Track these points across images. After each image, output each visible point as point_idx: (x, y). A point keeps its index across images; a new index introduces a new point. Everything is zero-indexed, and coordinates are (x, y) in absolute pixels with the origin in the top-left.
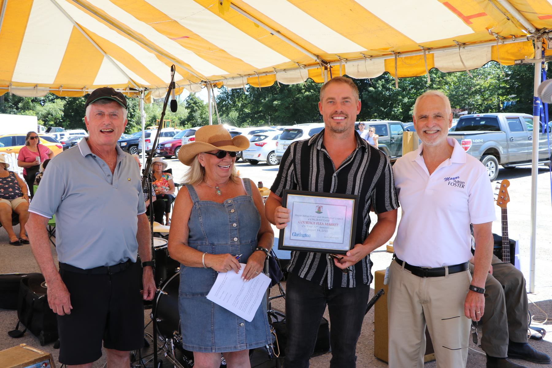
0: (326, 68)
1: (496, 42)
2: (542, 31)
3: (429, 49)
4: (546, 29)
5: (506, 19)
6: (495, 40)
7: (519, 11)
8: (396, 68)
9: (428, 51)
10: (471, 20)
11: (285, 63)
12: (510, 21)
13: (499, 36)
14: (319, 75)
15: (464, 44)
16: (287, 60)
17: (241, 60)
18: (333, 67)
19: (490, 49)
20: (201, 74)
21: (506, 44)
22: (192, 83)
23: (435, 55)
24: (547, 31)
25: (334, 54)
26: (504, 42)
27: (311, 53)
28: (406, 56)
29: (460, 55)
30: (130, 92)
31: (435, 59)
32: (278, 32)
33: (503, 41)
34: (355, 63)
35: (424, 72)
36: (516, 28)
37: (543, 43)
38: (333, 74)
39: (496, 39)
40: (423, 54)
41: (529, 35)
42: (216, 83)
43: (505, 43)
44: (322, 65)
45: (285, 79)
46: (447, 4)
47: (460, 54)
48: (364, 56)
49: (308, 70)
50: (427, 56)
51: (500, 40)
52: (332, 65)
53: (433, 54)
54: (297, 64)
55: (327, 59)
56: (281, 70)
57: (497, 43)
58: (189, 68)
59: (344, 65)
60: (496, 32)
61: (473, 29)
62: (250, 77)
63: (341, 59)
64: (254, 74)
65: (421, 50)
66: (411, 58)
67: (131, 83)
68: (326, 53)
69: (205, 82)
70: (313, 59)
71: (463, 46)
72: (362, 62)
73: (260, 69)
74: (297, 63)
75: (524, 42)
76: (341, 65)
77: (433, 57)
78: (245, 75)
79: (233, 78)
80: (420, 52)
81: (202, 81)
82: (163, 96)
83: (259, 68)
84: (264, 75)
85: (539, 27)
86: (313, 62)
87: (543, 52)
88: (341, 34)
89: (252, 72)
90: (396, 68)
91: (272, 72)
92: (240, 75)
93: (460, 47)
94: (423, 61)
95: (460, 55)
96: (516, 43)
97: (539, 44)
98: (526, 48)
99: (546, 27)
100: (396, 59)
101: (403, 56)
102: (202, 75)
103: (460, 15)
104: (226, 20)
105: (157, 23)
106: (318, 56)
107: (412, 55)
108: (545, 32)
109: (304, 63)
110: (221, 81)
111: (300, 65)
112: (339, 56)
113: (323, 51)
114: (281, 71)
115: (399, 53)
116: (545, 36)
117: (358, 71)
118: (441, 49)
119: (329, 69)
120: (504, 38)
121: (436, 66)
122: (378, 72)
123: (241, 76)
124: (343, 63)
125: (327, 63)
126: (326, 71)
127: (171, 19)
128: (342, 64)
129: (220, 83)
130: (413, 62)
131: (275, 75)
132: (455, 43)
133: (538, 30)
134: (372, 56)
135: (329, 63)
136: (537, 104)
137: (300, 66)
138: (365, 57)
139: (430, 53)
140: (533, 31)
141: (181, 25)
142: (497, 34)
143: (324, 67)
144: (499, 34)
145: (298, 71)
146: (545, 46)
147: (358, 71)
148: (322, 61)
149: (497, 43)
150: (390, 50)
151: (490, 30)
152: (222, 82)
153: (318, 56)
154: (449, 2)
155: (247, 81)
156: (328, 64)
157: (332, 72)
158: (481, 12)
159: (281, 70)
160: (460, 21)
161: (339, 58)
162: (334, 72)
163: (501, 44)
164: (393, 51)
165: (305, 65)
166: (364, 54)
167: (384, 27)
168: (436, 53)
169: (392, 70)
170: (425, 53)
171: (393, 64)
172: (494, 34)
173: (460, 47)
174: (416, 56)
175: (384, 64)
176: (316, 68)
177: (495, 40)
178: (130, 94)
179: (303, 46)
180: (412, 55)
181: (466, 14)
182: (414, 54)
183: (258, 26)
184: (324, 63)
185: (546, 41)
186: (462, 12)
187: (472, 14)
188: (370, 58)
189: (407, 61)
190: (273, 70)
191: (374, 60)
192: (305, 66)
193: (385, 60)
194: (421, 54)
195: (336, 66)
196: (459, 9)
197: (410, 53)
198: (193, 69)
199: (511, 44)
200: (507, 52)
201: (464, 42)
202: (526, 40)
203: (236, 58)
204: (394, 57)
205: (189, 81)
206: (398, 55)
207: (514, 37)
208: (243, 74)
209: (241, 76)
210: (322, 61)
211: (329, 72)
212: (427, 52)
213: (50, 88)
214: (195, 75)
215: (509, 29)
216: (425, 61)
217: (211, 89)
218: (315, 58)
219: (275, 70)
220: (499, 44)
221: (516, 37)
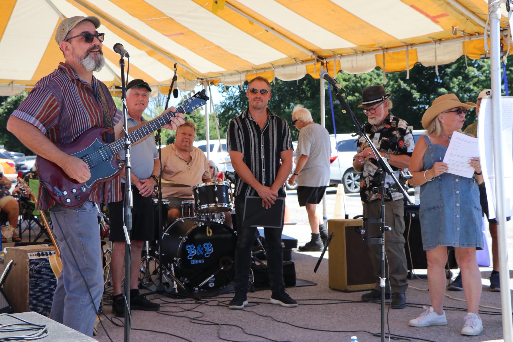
0: (322, 64)
1: (463, 38)
3: (412, 45)
5: (465, 19)
6: (461, 37)
7: (473, 13)
8: (384, 63)
9: (411, 46)
10: (438, 20)
11: (282, 59)
12: (468, 21)
13: (465, 33)
14: (312, 72)
15: (440, 40)
16: (284, 56)
17: (237, 56)
18: (330, 63)
19: (461, 45)
20: (196, 70)
21: (473, 40)
22: (187, 80)
23: (418, 50)
25: (328, 50)
26: (470, 38)
27: (306, 48)
28: (393, 51)
29: (435, 52)
30: (116, 91)
31: (418, 54)
32: (273, 29)
33: (469, 37)
34: (350, 59)
36: (475, 26)
38: (329, 69)
39: (463, 35)
40: (406, 49)
42: (213, 80)
43: (472, 39)
44: (318, 61)
45: (284, 75)
46: (412, 6)
47: (437, 50)
48: (355, 51)
49: (306, 66)
51: (466, 37)
52: (328, 60)
53: (416, 49)
54: (294, 60)
55: (324, 54)
56: (279, 66)
58: (184, 64)
59: (339, 61)
60: (462, 30)
61: (442, 27)
62: (249, 73)
63: (335, 55)
64: (253, 70)
65: (403, 46)
66: (398, 53)
67: (117, 80)
68: (321, 49)
69: (202, 79)
70: (309, 55)
71: (439, 42)
72: (354, 58)
73: (258, 66)
74: (295, 59)
76: (335, 61)
77: (416, 52)
78: (244, 72)
79: (231, 75)
80: (403, 48)
81: (198, 78)
82: (154, 95)
83: (257, 64)
84: (263, 71)
86: (309, 58)
88: (330, 31)
89: (249, 68)
90: (384, 63)
91: (270, 68)
92: (238, 71)
94: (406, 56)
95: (435, 52)
96: (479, 39)
100: (384, 54)
101: (390, 52)
102: (198, 71)
103: (427, 15)
104: (221, 18)
105: (152, 20)
106: (313, 52)
107: (398, 51)
109: (302, 59)
110: (218, 78)
111: (296, 61)
112: (333, 52)
113: (318, 47)
114: (279, 67)
115: (387, 48)
117: (352, 67)
118: (421, 45)
119: (325, 65)
120: (471, 35)
121: (419, 61)
122: (370, 67)
123: (239, 72)
124: (338, 59)
125: (322, 59)
126: (322, 66)
127: (166, 16)
128: (337, 59)
129: (217, 80)
131: (273, 71)
132: (432, 40)
134: (363, 52)
135: (325, 58)
137: (297, 62)
138: (356, 52)
139: (413, 48)
141: (176, 22)
142: (463, 31)
143: (320, 63)
144: (465, 32)
145: (295, 67)
146: (503, 42)
147: (352, 67)
148: (319, 57)
150: (376, 46)
151: (455, 28)
152: (220, 79)
153: (313, 52)
154: (416, 5)
155: (246, 78)
156: (324, 59)
157: (328, 68)
158: (444, 13)
159: (279, 66)
160: (428, 20)
161: (333, 53)
162: (331, 68)
163: (468, 40)
164: (381, 47)
165: (303, 61)
166: (355, 50)
167: (365, 25)
168: (419, 48)
169: (381, 65)
170: (407, 50)
171: (382, 60)
172: (457, 31)
175: (374, 60)
176: (313, 63)
177: (461, 37)
178: (116, 93)
179: (298, 42)
180: (398, 51)
181: (433, 14)
182: (399, 50)
183: (252, 24)
184: (320, 58)
185: (504, 38)
186: (428, 13)
187: (436, 15)
188: (363, 53)
189: (396, 56)
190: (271, 66)
191: (366, 56)
192: (303, 62)
193: (376, 55)
194: (404, 50)
195: (331, 61)
196: (425, 11)
197: (396, 49)
198: (188, 65)
199: (477, 40)
200: (474, 47)
201: (440, 38)
203: (232, 55)
204: (382, 53)
205: (184, 78)
206: (385, 50)
207: (477, 34)
208: (241, 70)
209: (239, 72)
210: (319, 57)
211: (326, 68)
212: (409, 48)
213: (27, 85)
214: (191, 71)
216: (408, 56)
217: (208, 87)
218: (311, 54)
219: (273, 66)
220: (465, 40)
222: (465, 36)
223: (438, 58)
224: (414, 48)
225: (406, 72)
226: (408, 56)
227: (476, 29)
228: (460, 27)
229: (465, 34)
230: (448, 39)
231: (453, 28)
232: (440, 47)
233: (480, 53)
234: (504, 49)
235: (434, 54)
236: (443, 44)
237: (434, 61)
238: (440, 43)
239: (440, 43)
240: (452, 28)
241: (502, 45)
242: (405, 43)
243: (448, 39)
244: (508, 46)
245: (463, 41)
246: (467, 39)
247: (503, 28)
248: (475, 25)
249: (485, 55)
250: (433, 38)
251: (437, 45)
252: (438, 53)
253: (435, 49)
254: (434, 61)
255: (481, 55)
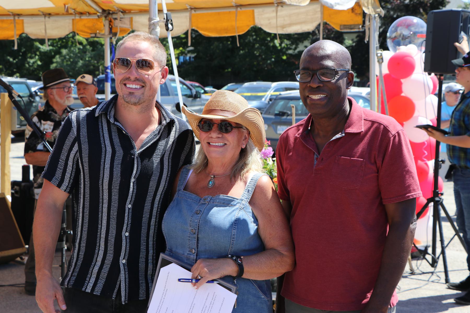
1: (74, 16)
2: (107, 12)
3: (19, 15)
4: (109, 10)
6: (71, 14)
13: (76, 11)
15: (50, 14)
19: (71, 21)
21: (83, 19)
24: (111, 12)
31: (25, 25)
33: (79, 16)
35: (13, 37)
37: (110, 21)
41: (99, 14)
43: (82, 18)
50: (16, 21)
51: (77, 15)
53: (23, 20)
57: (75, 17)
60: (73, 8)
61: (54, 4)
71: (48, 16)
75: (96, 19)
85: (105, 8)
87: (111, 29)
93: (45, 17)
94: (13, 25)
97: (107, 23)
98: (99, 23)
99: (110, 9)
108: (109, 13)
116: (110, 16)
120: (81, 14)
130: (5, 25)
132: (41, 14)
133: (104, 11)
136: (107, 72)
140: (100, 11)
142: (74, 9)
146: (111, 24)
149: (75, 17)
168: (26, 20)
170: (14, 20)
173: (45, 17)
174: (7, 20)
177: (71, 14)
182: (5, 18)
185: (113, 20)
199: (87, 19)
200: (84, 25)
202: (97, 17)
207: (87, 14)
212: (16, 18)
215: (81, 7)
216: (15, 26)
221: (89, 14)
222: (76, 14)
223: (48, 31)
224: (21, 18)
225: (13, 41)
226: (15, 26)
227: (86, 9)
228: (71, 5)
229: (76, 12)
230: (57, 14)
231: (65, 5)
232: (50, 22)
233: (90, 32)
234: (114, 31)
235: (43, 27)
236: (52, 18)
237: (44, 34)
238: (49, 17)
239: (49, 17)
240: (63, 6)
241: (110, 27)
242: (12, 13)
243: (57, 14)
244: (117, 28)
245: (74, 18)
246: (77, 17)
247: (112, 11)
248: (87, 5)
249: (96, 34)
250: (43, 12)
251: (47, 18)
252: (47, 26)
253: (45, 22)
254: (44, 34)
255: (91, 34)
